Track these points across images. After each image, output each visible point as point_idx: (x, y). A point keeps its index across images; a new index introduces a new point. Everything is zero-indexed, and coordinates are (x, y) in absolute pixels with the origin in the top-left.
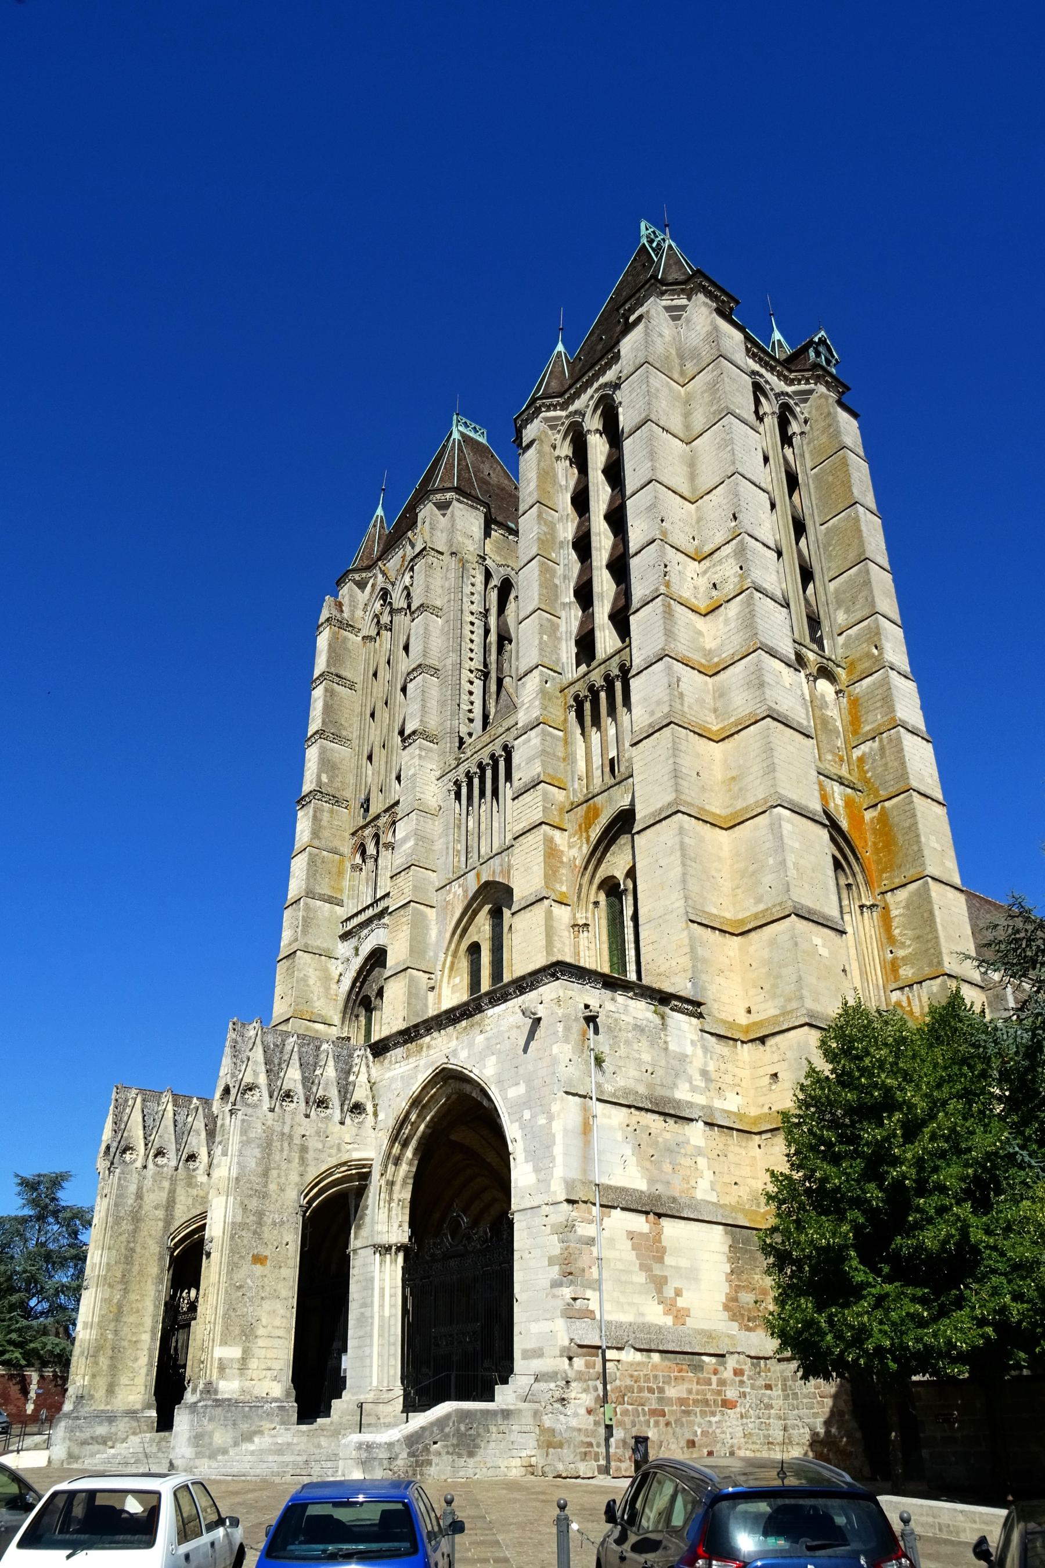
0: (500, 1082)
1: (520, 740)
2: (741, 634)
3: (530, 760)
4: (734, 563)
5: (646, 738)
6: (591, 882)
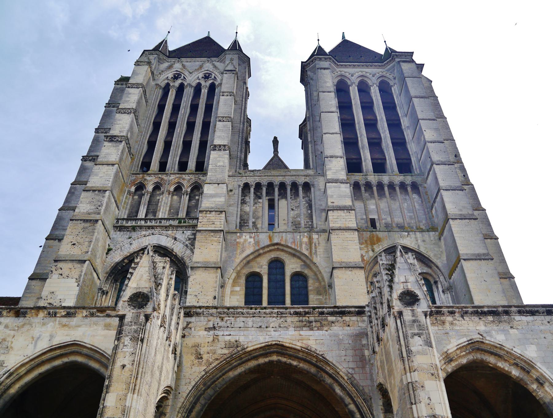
0: (544, 363)
1: (330, 184)
3: (340, 196)
5: (460, 219)
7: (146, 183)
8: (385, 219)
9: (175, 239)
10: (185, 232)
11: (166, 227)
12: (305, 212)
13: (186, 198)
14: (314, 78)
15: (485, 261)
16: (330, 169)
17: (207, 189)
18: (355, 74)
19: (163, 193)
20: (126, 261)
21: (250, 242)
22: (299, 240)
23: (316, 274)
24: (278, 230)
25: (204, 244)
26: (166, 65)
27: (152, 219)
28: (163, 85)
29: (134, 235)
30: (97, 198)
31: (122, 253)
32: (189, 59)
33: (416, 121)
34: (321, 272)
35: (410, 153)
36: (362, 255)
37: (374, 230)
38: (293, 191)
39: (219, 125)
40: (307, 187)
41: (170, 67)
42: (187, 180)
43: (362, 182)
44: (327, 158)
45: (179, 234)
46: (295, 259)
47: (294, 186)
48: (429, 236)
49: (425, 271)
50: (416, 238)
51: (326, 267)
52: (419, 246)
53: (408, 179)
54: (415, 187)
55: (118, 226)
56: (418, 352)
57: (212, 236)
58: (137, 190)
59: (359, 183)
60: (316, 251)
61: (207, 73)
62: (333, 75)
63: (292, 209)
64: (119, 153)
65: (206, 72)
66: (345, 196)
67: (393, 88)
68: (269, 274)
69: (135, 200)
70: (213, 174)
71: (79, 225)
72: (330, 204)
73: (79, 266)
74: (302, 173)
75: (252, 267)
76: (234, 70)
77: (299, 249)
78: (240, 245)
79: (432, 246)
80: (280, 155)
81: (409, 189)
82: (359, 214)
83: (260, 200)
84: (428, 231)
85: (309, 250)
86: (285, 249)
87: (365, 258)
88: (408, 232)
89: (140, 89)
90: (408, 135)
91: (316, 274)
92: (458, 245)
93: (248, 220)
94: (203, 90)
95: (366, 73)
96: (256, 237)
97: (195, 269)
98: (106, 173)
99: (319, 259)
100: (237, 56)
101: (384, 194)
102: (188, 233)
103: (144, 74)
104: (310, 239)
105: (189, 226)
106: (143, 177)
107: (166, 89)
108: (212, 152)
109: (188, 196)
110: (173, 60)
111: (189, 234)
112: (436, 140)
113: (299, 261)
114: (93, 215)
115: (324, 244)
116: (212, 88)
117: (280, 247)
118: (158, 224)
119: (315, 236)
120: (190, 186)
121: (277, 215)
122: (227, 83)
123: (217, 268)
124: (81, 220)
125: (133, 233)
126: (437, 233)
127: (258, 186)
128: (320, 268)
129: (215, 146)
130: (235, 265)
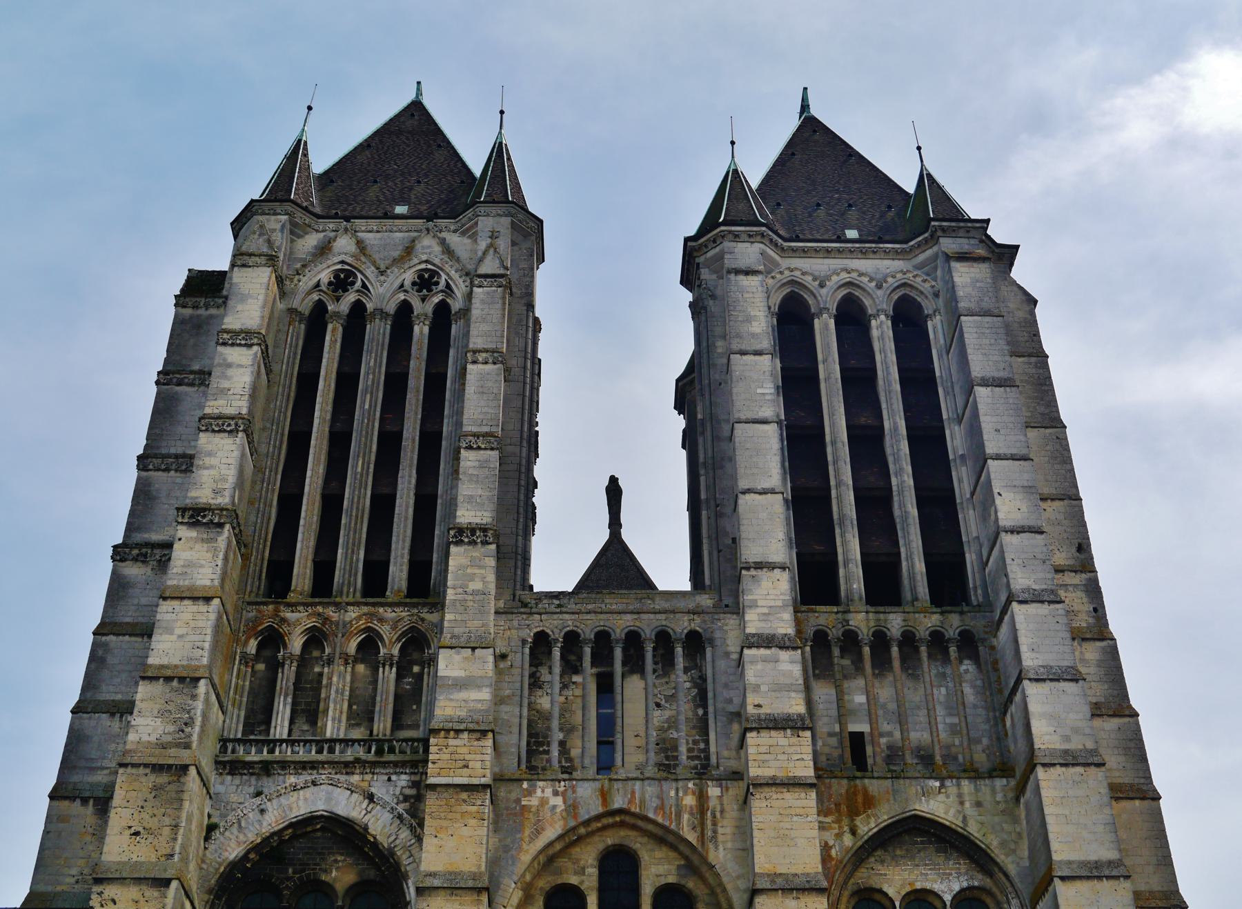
1: (754, 651)
2: (1106, 687)
3: (779, 688)
4: (1085, 600)
5: (1062, 765)
6: (846, 883)
7: (285, 628)
8: (890, 734)
9: (371, 798)
10: (394, 778)
11: (346, 764)
12: (690, 714)
13: (388, 676)
14: (719, 292)
15: (1112, 882)
16: (754, 605)
17: (449, 665)
18: (828, 278)
19: (330, 662)
20: (252, 856)
21: (555, 807)
22: (673, 802)
23: (713, 893)
24: (622, 774)
25: (444, 823)
26: (311, 241)
27: (311, 741)
28: (305, 307)
29: (269, 785)
30: (179, 700)
31: (241, 837)
32: (373, 224)
33: (980, 460)
34: (724, 890)
35: (964, 539)
36: (826, 843)
37: (859, 774)
38: (661, 651)
39: (469, 459)
40: (696, 643)
41: (324, 250)
42: (391, 622)
43: (835, 633)
44: (748, 569)
45: (379, 787)
46: (664, 849)
47: (664, 639)
48: (994, 792)
49: (976, 884)
50: (960, 796)
51: (738, 877)
52: (965, 818)
53: (953, 624)
54: (969, 644)
55: (227, 762)
57: (464, 801)
58: (260, 647)
59: (826, 634)
60: (715, 832)
61: (426, 270)
62: (770, 281)
63: (658, 705)
64: (220, 563)
65: (423, 266)
66: (789, 688)
67: (930, 324)
68: (602, 890)
69: (259, 675)
70: (459, 617)
71: (144, 779)
72: (750, 709)
73: (156, 894)
74: (681, 604)
75: (559, 872)
76: (502, 276)
77: (673, 827)
78: (531, 816)
79: (997, 819)
80: (626, 535)
81: (953, 650)
82: (825, 720)
83: (576, 678)
84: (991, 777)
85: (699, 829)
86: (640, 823)
87: (833, 853)
88: (942, 779)
89: (256, 348)
90: (962, 480)
91: (713, 893)
92: (1051, 836)
93: (546, 737)
94: (416, 329)
95: (861, 275)
96: (570, 792)
97: (427, 892)
98: (192, 624)
99: (721, 856)
100: (506, 221)
101: (889, 661)
102: (403, 780)
103: (261, 297)
104: (702, 797)
105: (403, 764)
106: (277, 611)
107: (317, 319)
108: (453, 549)
109: (394, 669)
110: (331, 224)
111: (404, 783)
112: (1026, 523)
113: (672, 854)
114: (173, 752)
115: (735, 814)
116: (442, 317)
117: (627, 819)
118: (324, 756)
119: (713, 791)
120: (398, 640)
121: (619, 713)
122: (484, 320)
123: (479, 890)
124: (146, 766)
125: (265, 779)
126: (1013, 783)
127: (572, 639)
128: (725, 879)
129: (461, 531)
130: (520, 868)
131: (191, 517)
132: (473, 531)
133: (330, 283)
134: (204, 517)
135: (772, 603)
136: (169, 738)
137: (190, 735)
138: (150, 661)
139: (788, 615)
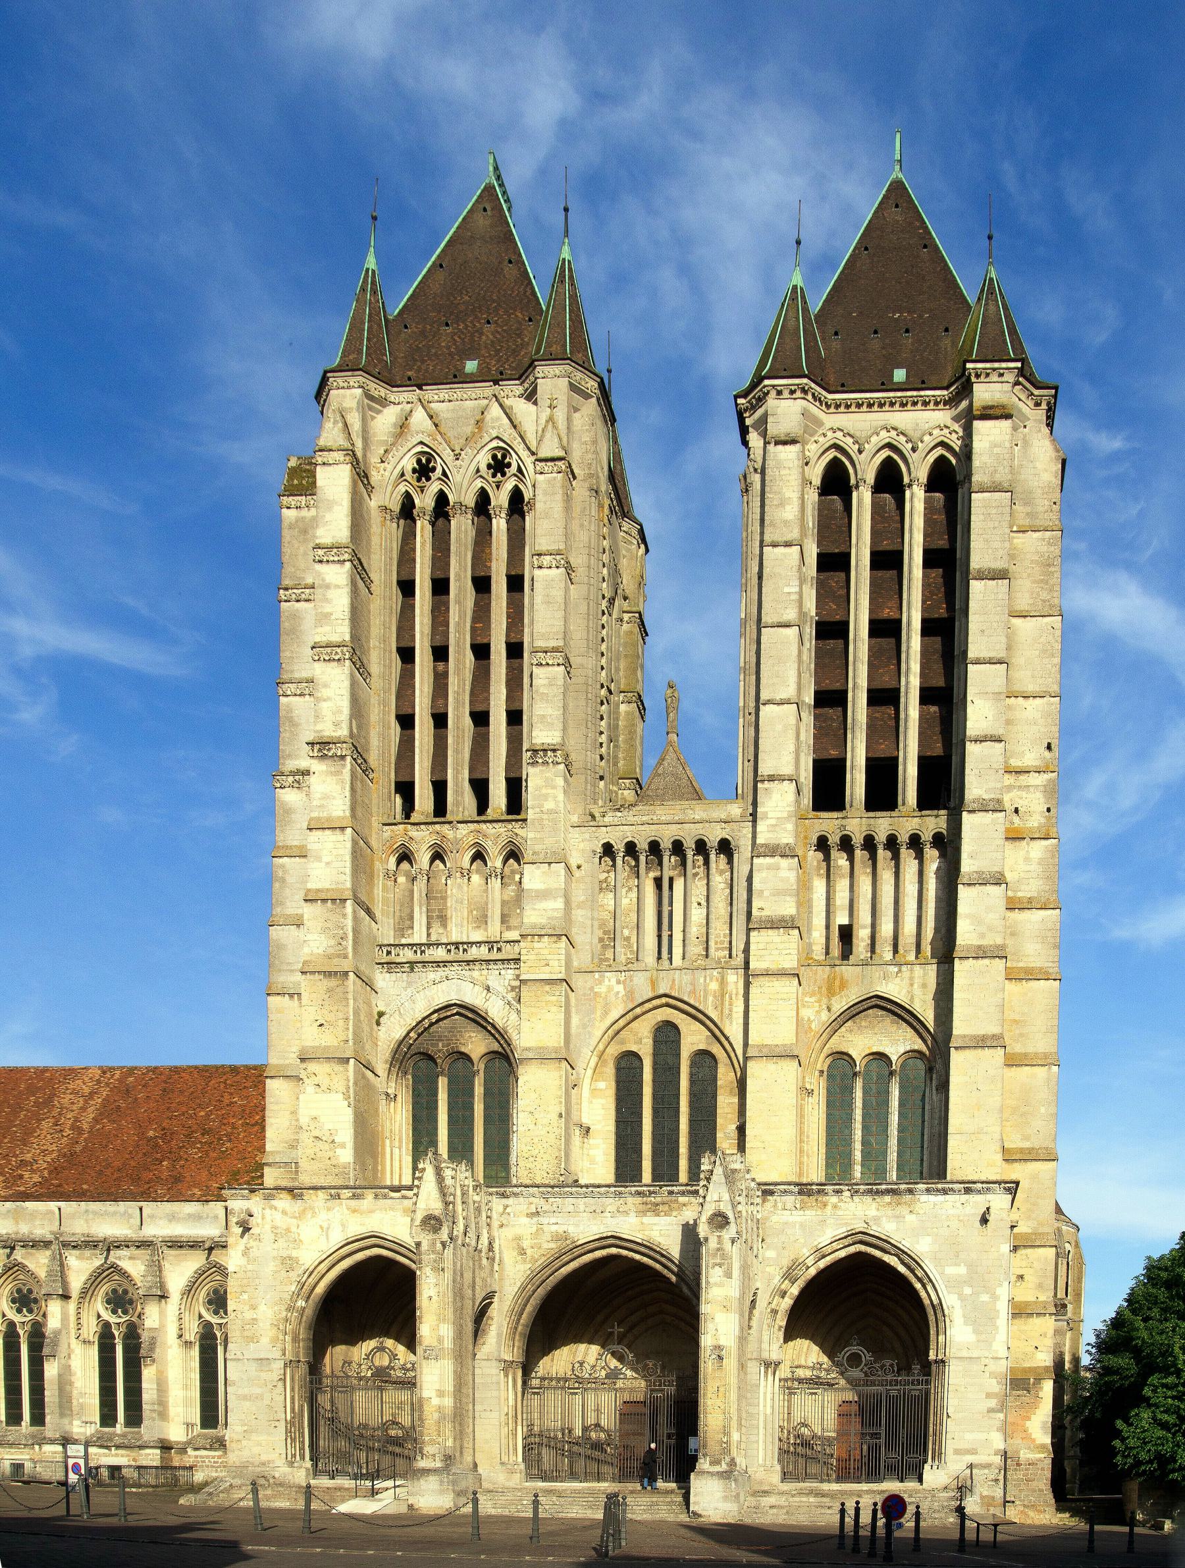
16: (766, 817)
56: (716, 1284)
129: (535, 751)
131: (320, 750)
132: (545, 750)
133: (414, 471)
134: (329, 750)
135: (780, 815)
136: (331, 951)
137: (346, 948)
138: (309, 886)
139: (790, 827)
